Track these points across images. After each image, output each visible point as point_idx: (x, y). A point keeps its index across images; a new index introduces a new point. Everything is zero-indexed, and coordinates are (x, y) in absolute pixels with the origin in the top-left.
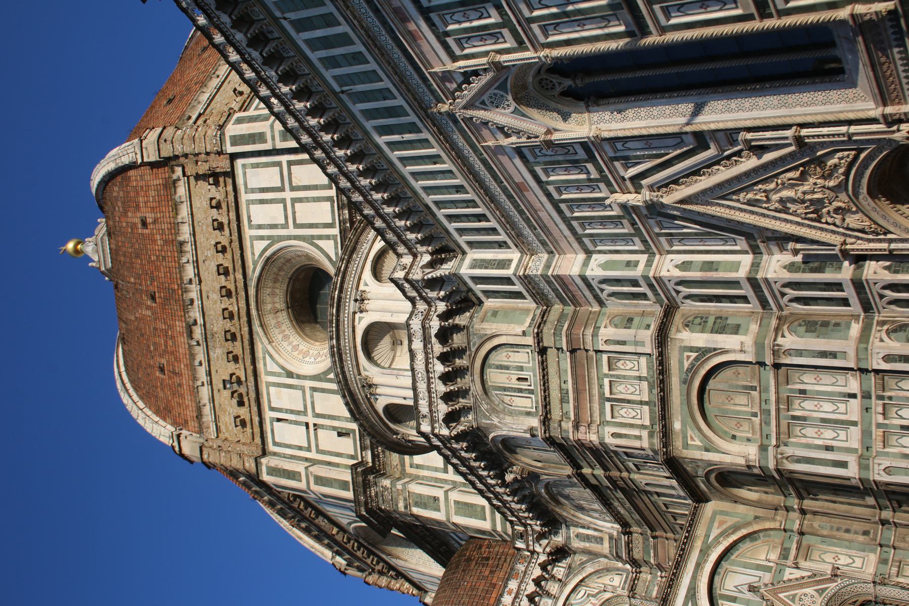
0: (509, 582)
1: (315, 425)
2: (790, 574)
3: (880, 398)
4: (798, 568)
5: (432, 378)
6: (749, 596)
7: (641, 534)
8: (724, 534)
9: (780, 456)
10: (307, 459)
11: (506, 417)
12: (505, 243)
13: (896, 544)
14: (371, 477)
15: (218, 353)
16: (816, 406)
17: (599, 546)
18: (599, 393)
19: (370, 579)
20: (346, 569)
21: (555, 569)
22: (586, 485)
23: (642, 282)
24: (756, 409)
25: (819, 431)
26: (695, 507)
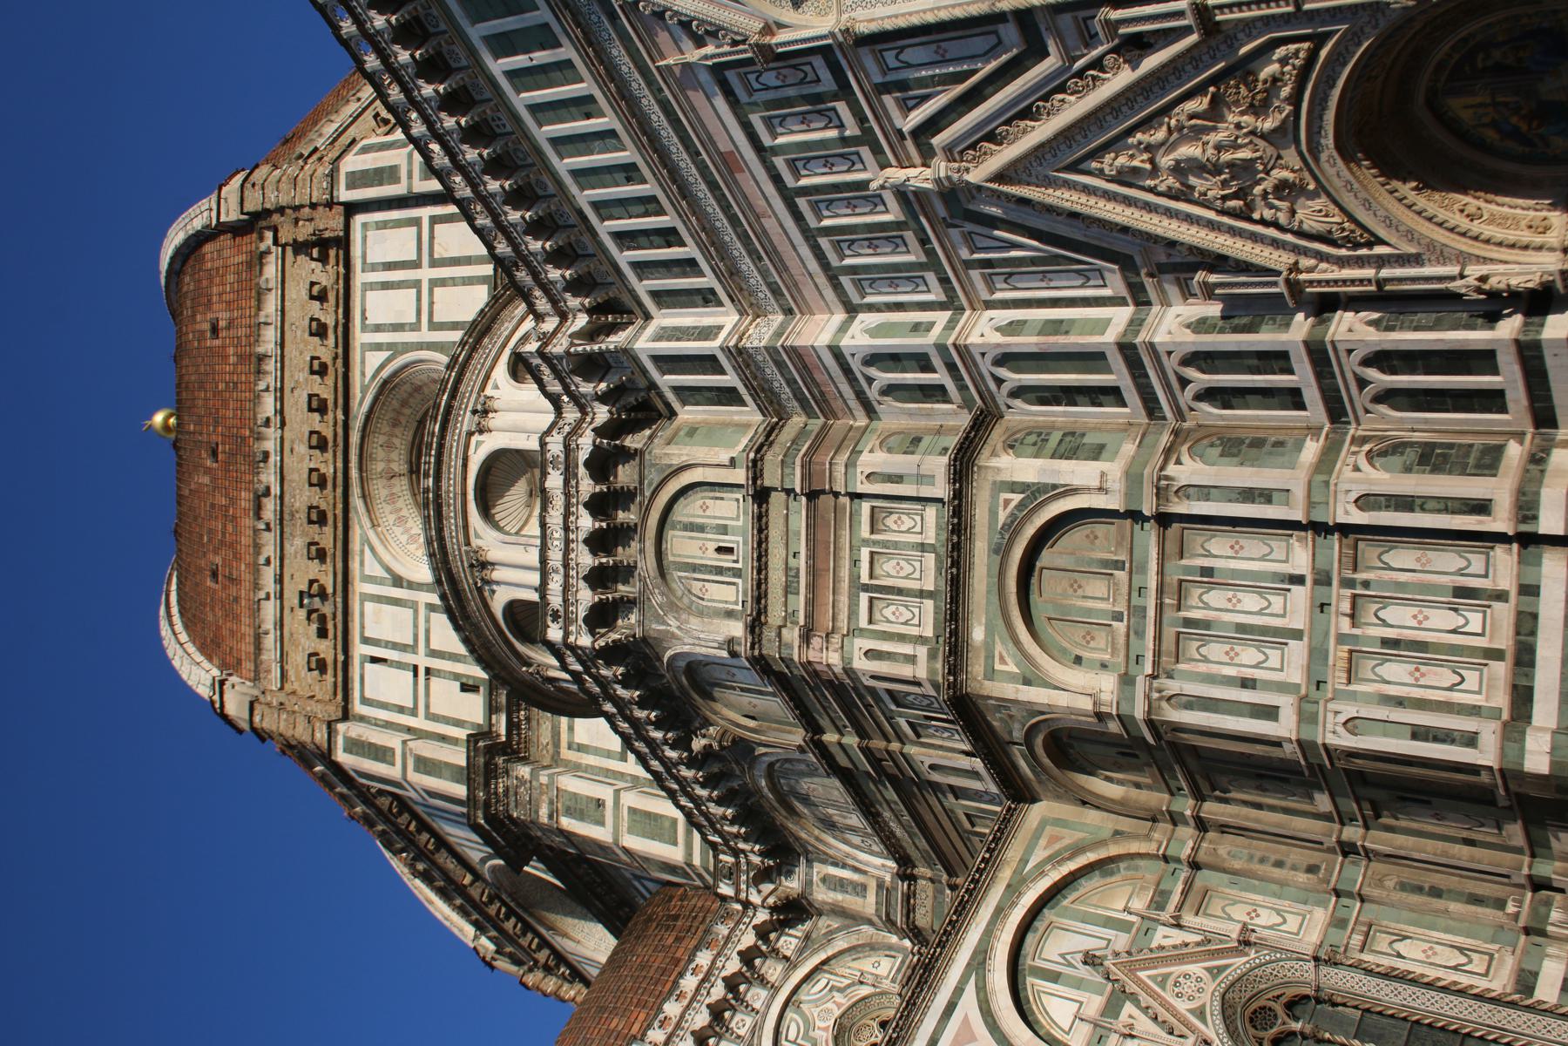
0: (699, 953)
1: (428, 671)
2: (1165, 937)
3: (1348, 583)
4: (1179, 926)
5: (573, 541)
6: (1084, 972)
7: (932, 880)
8: (1055, 859)
9: (1155, 695)
10: (409, 730)
12: (712, 291)
13: (1366, 891)
14: (500, 760)
15: (296, 545)
16: (1230, 600)
17: (859, 900)
18: (851, 575)
19: (530, 979)
20: (493, 958)
21: (783, 938)
22: (830, 766)
23: (937, 361)
24: (1121, 607)
25: (1232, 649)
26: (1010, 808)
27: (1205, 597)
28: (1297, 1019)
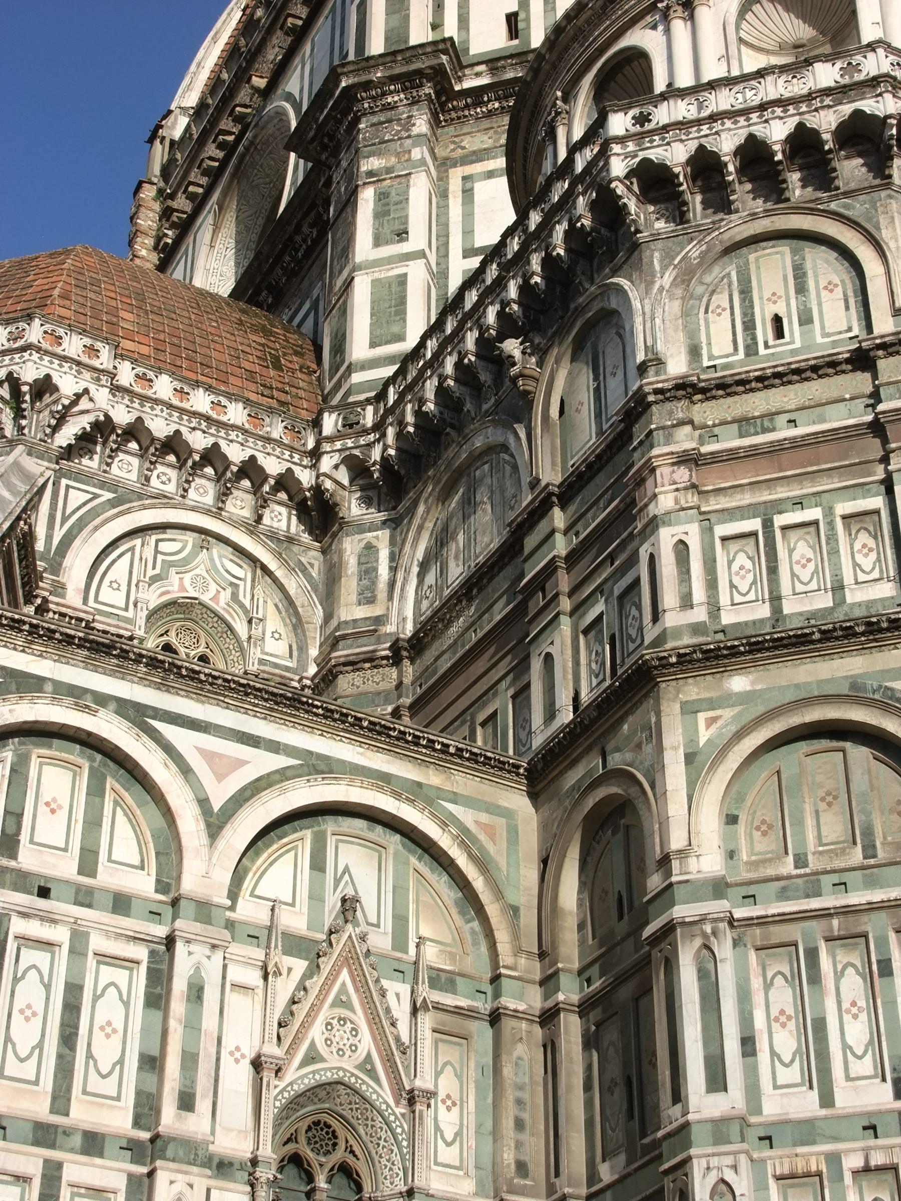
0: (240, 405)
2: (398, 995)
4: (415, 1011)
5: (748, 120)
6: (332, 902)
7: (400, 685)
9: (708, 928)
11: (677, 304)
14: (428, 89)
16: (854, 1004)
17: (354, 598)
19: (148, 193)
20: (163, 138)
21: (283, 510)
22: (520, 526)
24: (814, 864)
25: (789, 1018)
26: (518, 767)
27: (850, 971)
28: (329, 1181)
